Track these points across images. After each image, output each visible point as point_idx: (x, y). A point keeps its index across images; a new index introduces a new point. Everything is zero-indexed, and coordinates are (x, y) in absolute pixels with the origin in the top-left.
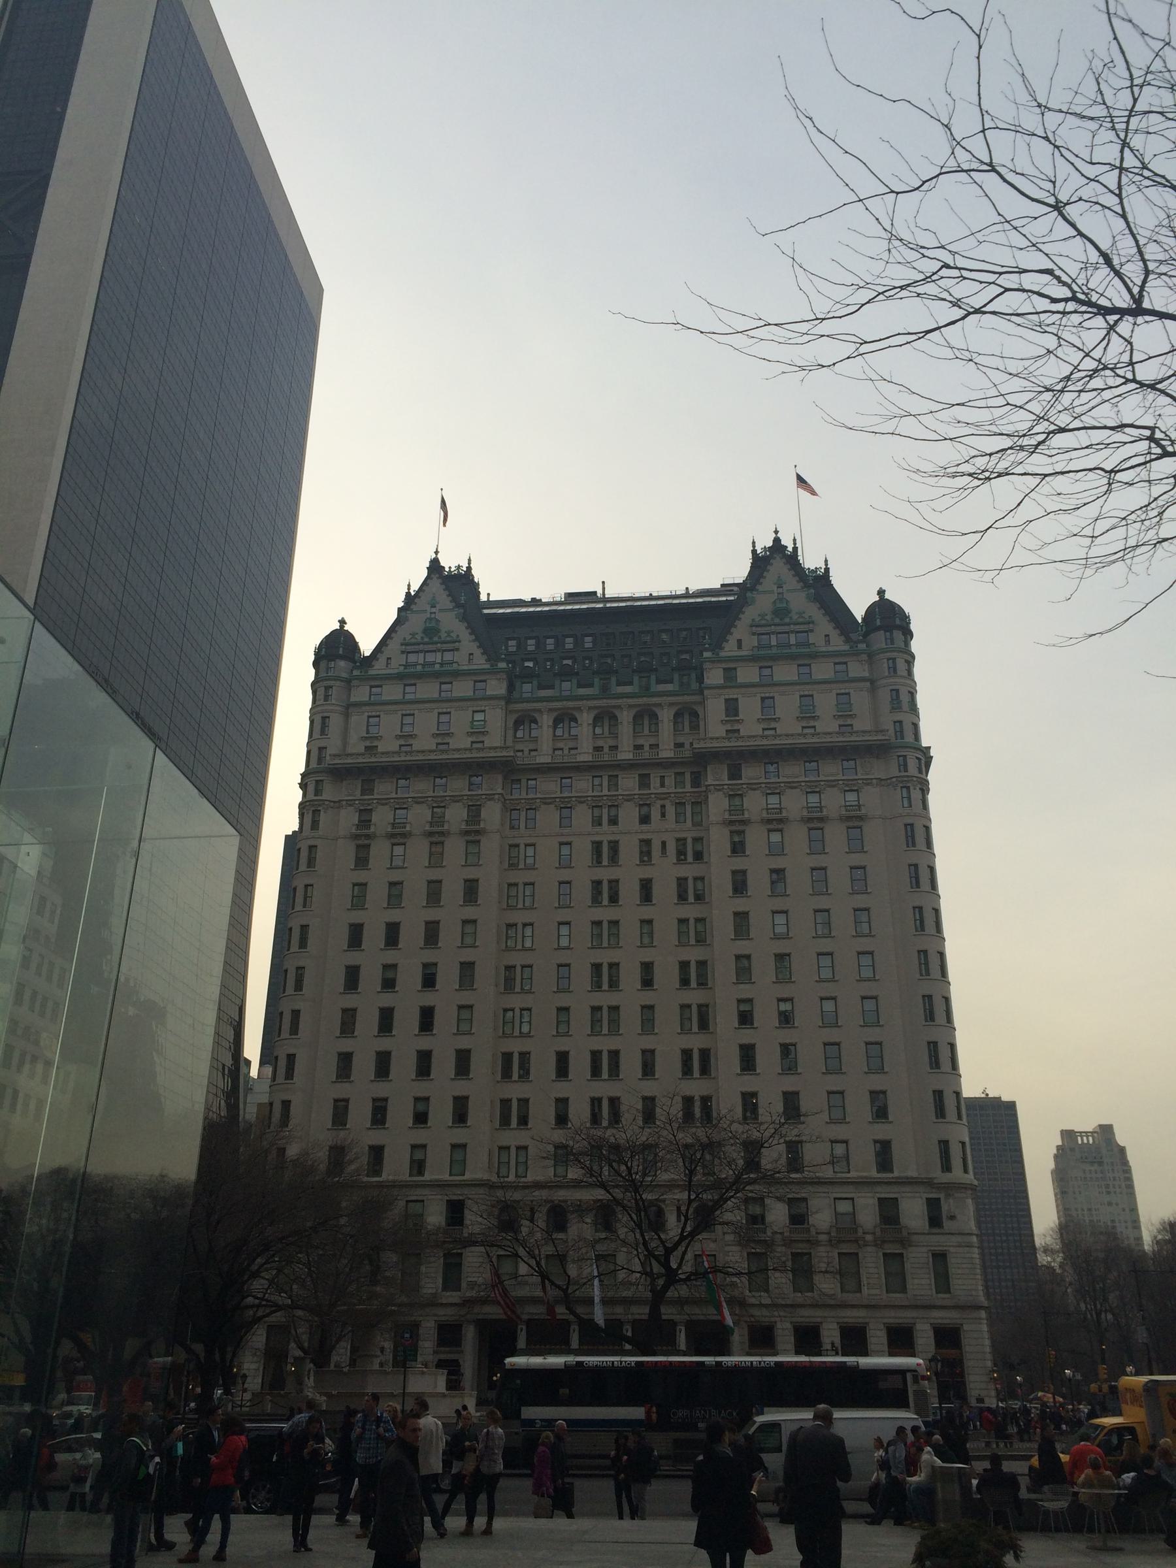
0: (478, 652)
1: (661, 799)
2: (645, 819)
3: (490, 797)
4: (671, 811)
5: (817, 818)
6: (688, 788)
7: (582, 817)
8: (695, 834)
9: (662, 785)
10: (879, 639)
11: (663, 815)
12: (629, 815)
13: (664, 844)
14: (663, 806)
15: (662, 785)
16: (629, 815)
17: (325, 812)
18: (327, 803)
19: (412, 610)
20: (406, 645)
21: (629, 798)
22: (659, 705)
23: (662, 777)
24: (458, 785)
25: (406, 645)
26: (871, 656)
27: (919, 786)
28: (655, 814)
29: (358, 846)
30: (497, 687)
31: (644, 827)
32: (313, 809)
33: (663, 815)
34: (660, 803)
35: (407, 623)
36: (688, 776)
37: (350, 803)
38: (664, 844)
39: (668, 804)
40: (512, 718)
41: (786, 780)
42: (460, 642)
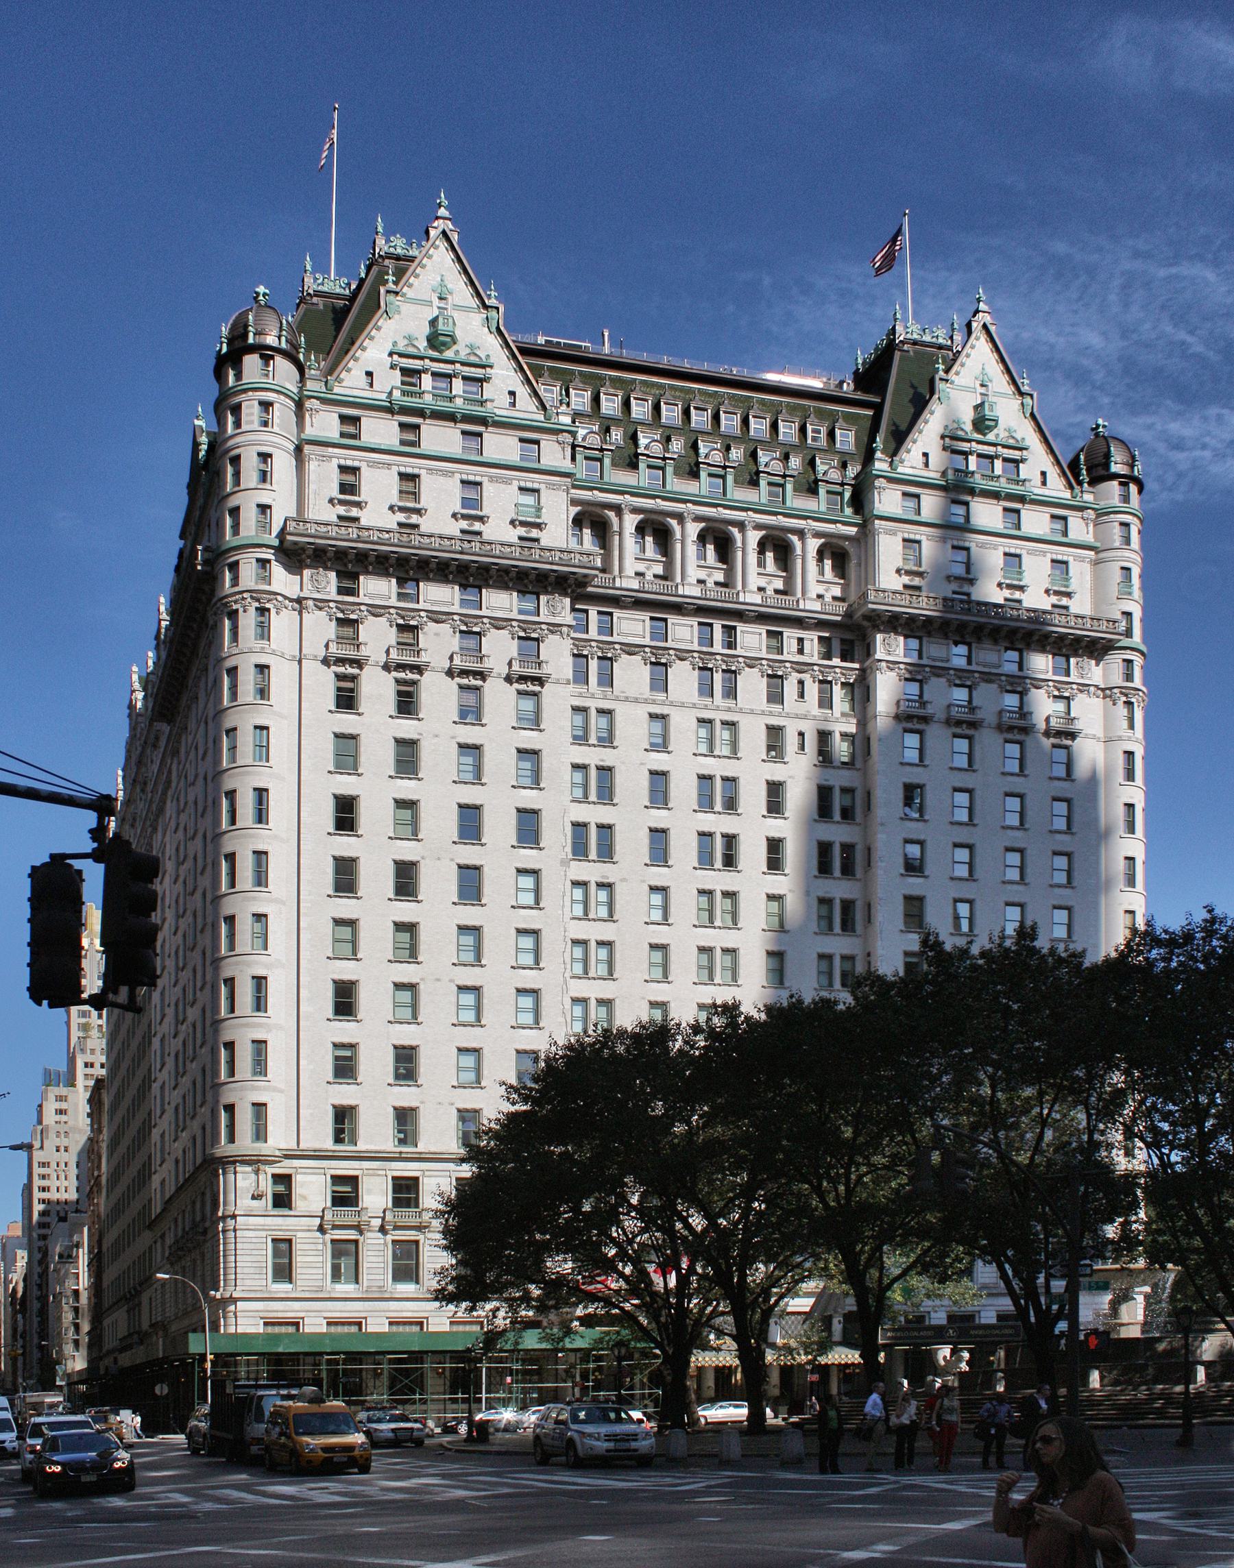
0: (523, 392)
1: (799, 672)
2: (776, 696)
3: (555, 628)
4: (812, 689)
5: (918, 717)
7: (683, 678)
9: (801, 651)
11: (802, 695)
12: (752, 685)
14: (801, 682)
15: (801, 651)
16: (752, 685)
17: (277, 613)
18: (280, 598)
19: (404, 295)
20: (401, 355)
21: (752, 662)
23: (801, 640)
24: (500, 602)
25: (401, 355)
27: (1124, 699)
28: (790, 688)
32: (257, 605)
34: (795, 676)
35: (396, 316)
37: (321, 604)
39: (806, 677)
40: (574, 510)
41: (980, 669)
42: (491, 367)
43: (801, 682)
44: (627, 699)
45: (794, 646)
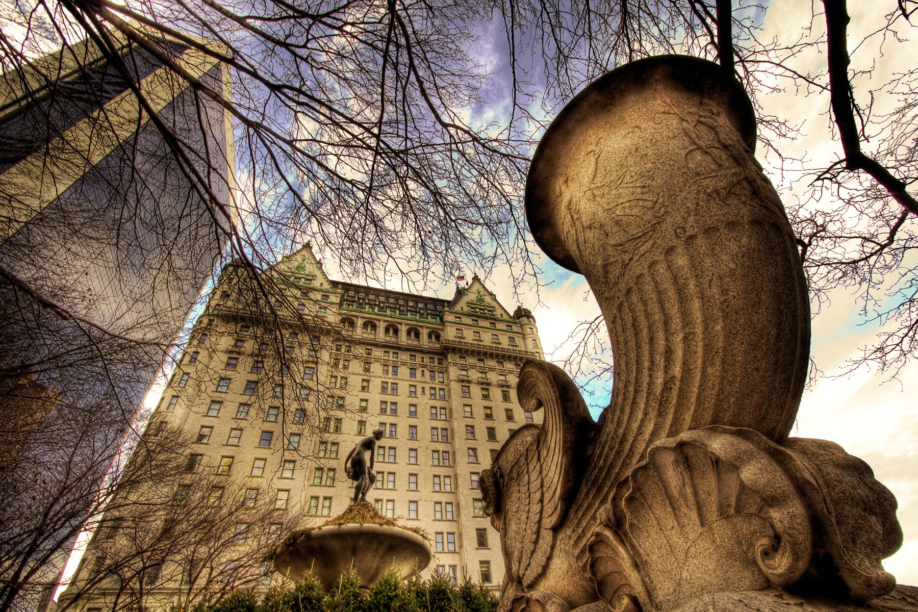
6: (436, 364)
8: (441, 387)
9: (423, 361)
10: (524, 320)
11: (423, 375)
13: (423, 388)
14: (423, 371)
15: (423, 361)
22: (422, 327)
26: (522, 326)
28: (419, 373)
29: (230, 358)
30: (334, 298)
31: (413, 379)
33: (423, 375)
34: (421, 369)
36: (436, 360)
38: (423, 388)
43: (423, 371)
44: (353, 374)
45: (420, 359)
